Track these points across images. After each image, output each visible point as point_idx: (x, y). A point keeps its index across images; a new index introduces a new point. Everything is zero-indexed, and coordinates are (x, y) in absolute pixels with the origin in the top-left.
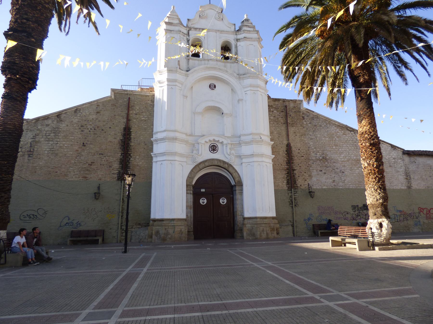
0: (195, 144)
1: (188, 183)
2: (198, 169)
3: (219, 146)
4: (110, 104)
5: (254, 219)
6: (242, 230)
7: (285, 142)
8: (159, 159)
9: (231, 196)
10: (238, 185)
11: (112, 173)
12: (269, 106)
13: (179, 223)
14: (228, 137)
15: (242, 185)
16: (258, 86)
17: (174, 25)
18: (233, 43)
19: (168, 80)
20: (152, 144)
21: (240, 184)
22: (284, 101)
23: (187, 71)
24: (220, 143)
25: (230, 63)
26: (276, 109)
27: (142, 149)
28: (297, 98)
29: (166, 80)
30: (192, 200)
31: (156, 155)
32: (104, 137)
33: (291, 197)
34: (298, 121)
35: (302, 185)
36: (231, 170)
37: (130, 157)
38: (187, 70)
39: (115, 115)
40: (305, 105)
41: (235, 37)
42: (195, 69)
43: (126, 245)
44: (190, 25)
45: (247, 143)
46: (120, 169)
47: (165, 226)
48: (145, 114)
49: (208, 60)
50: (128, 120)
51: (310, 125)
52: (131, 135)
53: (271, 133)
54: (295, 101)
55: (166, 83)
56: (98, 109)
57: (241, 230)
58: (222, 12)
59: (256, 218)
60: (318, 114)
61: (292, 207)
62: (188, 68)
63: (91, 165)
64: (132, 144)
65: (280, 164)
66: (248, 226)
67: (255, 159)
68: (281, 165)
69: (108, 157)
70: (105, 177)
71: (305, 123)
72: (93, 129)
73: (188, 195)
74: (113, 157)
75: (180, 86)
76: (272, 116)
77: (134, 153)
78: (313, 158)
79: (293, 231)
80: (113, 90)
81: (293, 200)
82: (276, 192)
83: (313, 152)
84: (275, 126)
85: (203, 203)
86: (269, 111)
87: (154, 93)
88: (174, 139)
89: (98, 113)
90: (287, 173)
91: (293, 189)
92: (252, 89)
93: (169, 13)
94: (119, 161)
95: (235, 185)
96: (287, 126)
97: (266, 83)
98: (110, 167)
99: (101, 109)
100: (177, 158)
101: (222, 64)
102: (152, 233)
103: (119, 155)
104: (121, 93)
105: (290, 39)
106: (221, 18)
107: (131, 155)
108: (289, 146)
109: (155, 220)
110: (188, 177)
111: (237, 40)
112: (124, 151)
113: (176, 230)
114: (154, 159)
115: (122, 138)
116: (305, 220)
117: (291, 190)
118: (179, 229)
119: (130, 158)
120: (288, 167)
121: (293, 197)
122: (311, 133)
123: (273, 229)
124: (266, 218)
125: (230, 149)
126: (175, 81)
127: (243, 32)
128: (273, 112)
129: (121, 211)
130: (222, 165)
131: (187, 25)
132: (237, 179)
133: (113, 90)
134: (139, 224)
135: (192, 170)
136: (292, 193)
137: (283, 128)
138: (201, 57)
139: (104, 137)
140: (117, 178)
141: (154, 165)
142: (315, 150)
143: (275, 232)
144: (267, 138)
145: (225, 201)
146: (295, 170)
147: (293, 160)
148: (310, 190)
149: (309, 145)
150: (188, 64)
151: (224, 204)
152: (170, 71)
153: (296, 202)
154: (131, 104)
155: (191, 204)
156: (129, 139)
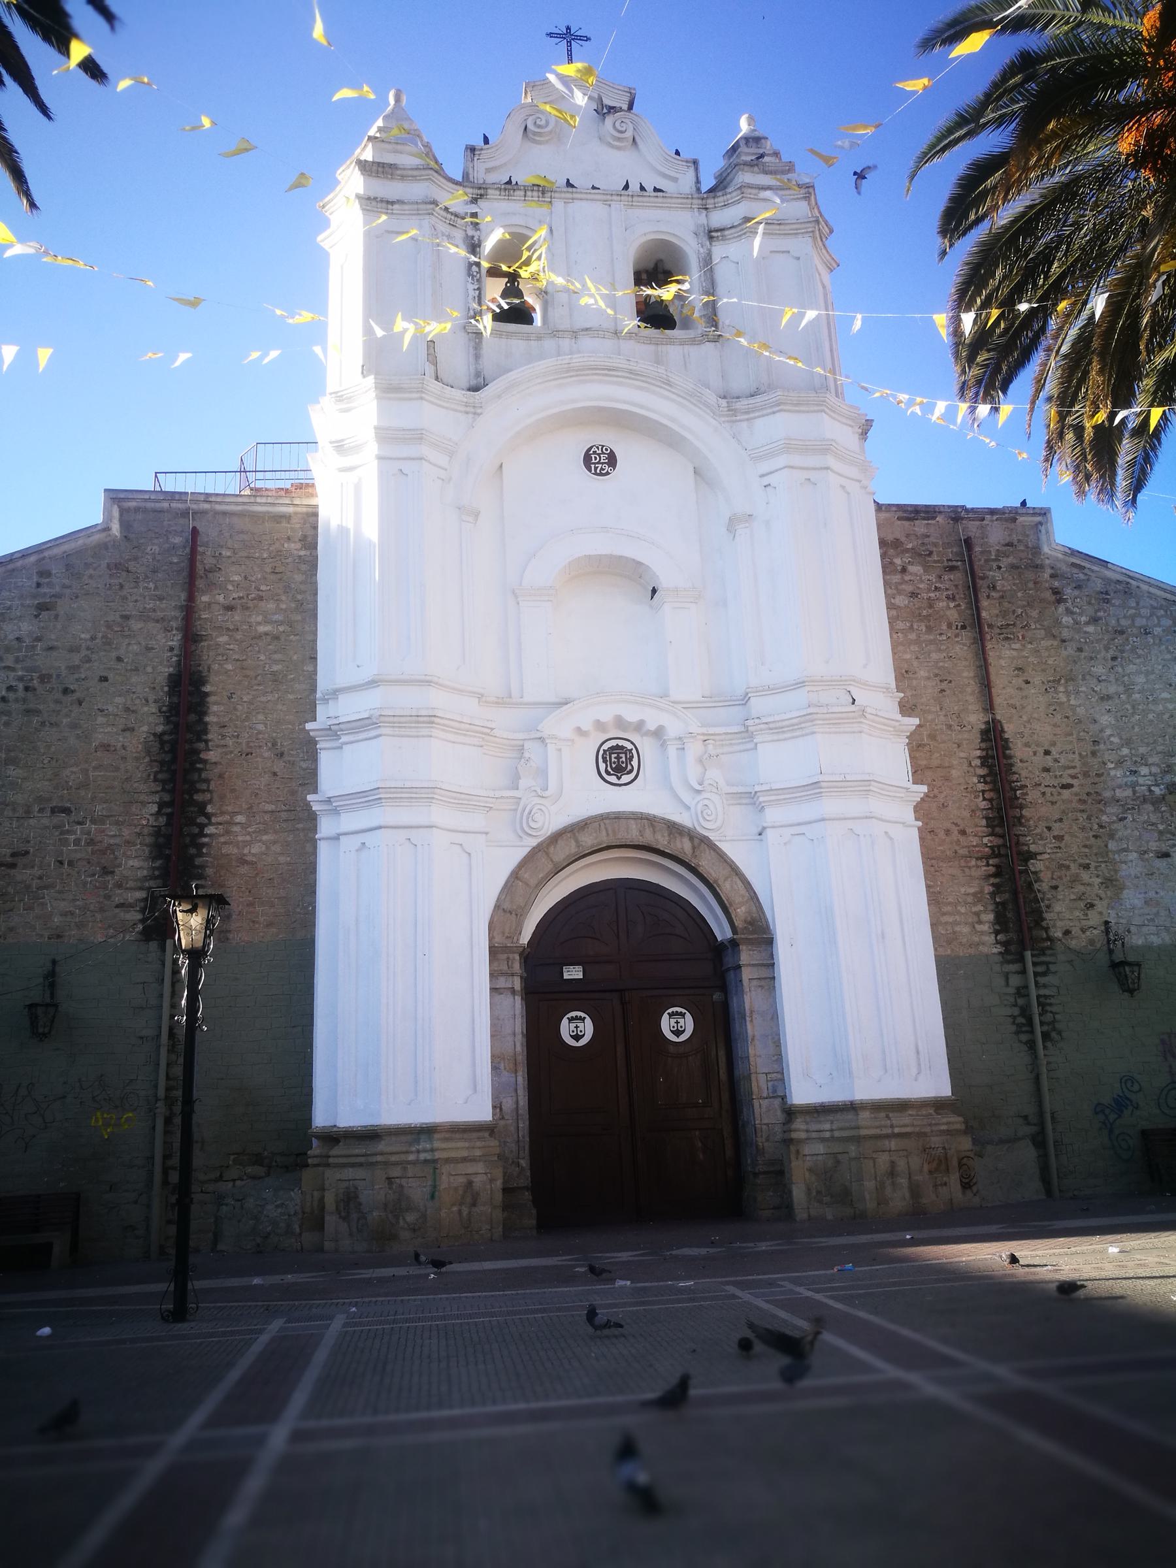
0: (527, 745)
1: (498, 939)
2: (546, 866)
3: (647, 748)
4: (104, 564)
5: (839, 1116)
6: (781, 1173)
7: (976, 719)
8: (349, 821)
9: (717, 996)
10: (749, 942)
11: (117, 900)
12: (883, 543)
13: (459, 1148)
14: (689, 706)
15: (770, 942)
16: (825, 448)
17: (403, 178)
18: (692, 248)
19: (385, 435)
22: (957, 515)
23: (475, 389)
24: (649, 733)
25: (683, 343)
26: (922, 555)
27: (266, 779)
29: (371, 434)
30: (517, 1025)
31: (334, 806)
32: (74, 726)
33: (1022, 992)
34: (1035, 614)
35: (1076, 931)
36: (706, 864)
37: (202, 820)
38: (473, 382)
39: (126, 618)
41: (702, 219)
42: (512, 375)
43: (181, 1275)
44: (479, 173)
45: (782, 729)
46: (152, 883)
47: (386, 1163)
48: (271, 606)
49: (575, 334)
50: (191, 637)
51: (1090, 629)
52: (205, 713)
53: (903, 674)
54: (1007, 516)
55: (372, 448)
56: (45, 590)
57: (779, 1174)
58: (630, 107)
59: (852, 1107)
60: (1130, 576)
61: (1031, 1045)
62: (478, 374)
63: (13, 866)
64: (212, 756)
65: (955, 830)
66: (815, 1150)
67: (830, 806)
68: (963, 832)
69: (93, 821)
70: (80, 926)
71: (1067, 620)
72: (21, 686)
73: (498, 998)
74: (117, 823)
75: (443, 460)
76: (900, 592)
77: (222, 797)
78: (1119, 793)
79: (1044, 1169)
80: (115, 497)
81: (1036, 1010)
83: (1120, 763)
84: (917, 642)
85: (577, 1038)
86: (884, 567)
87: (313, 502)
88: (422, 722)
89: (42, 607)
90: (995, 875)
91: (1028, 954)
92: (797, 460)
93: (380, 123)
94: (148, 840)
95: (734, 944)
96: (980, 641)
97: (864, 434)
98: (107, 871)
99: (58, 589)
100: (439, 814)
102: (322, 1199)
103: (147, 813)
104: (155, 511)
105: (990, 182)
106: (629, 134)
107: (209, 809)
108: (994, 740)
109: (333, 1137)
110: (497, 907)
112: (172, 792)
113: (444, 1182)
114: (326, 827)
115: (160, 729)
116: (1099, 1109)
117: (1022, 959)
118: (462, 1180)
119: (202, 827)
120: (999, 841)
121: (1033, 993)
122: (1099, 670)
123: (940, 1164)
124: (901, 1106)
125: (700, 761)
126: (417, 436)
127: (735, 196)
128: (904, 570)
129: (161, 1093)
130: (662, 841)
131: (466, 175)
132: (741, 913)
133: (115, 497)
134: (258, 1160)
135: (515, 875)
136: (1023, 972)
137: (962, 647)
138: (538, 317)
139: (74, 726)
140: (140, 927)
141: (324, 853)
142: (1125, 751)
143: (954, 1179)
144: (881, 698)
145: (688, 1024)
146: (1033, 856)
147: (1021, 807)
148: (1119, 957)
149: (1094, 728)
150: (477, 357)
151: (683, 1038)
152: (389, 390)
153: (1048, 1017)
154: (207, 559)
155: (517, 1044)
156: (199, 731)
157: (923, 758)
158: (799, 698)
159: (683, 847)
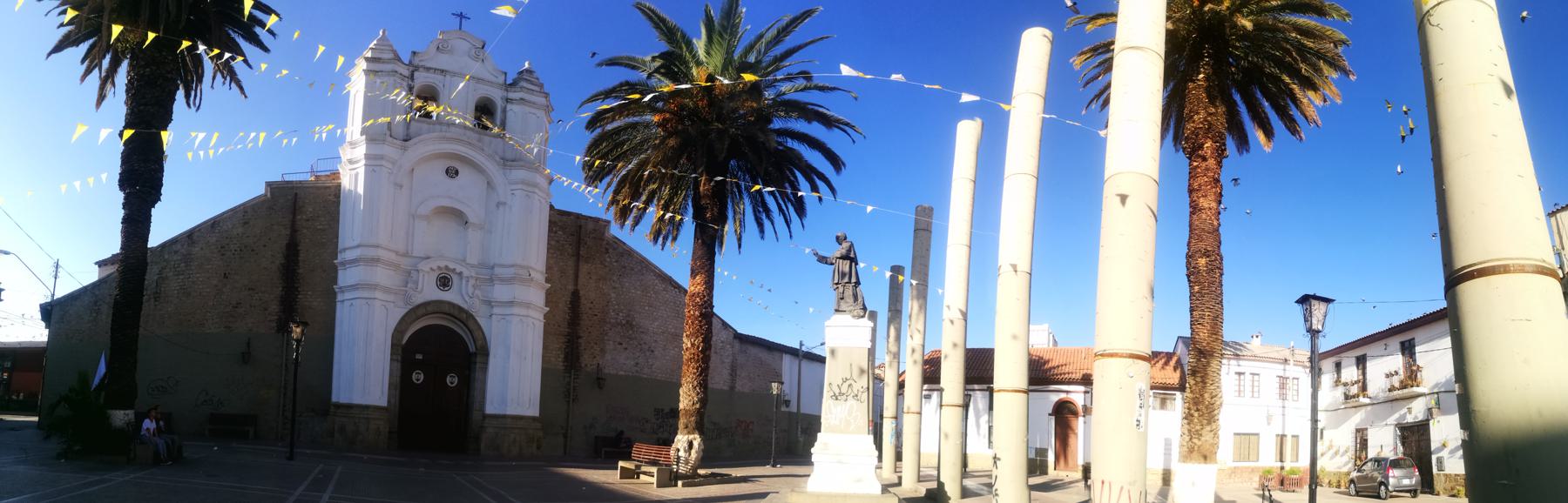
7: (571, 287)
18: (499, 103)
20: (335, 269)
21: (484, 352)
22: (578, 216)
28: (604, 217)
30: (398, 373)
31: (342, 290)
40: (614, 230)
53: (549, 268)
54: (597, 220)
67: (516, 310)
82: (546, 373)
101: (473, 137)
111: (508, 100)
114: (339, 297)
126: (381, 157)
137: (571, 263)
145: (456, 380)
157: (550, 298)
158: (512, 270)
159: (463, 316)
